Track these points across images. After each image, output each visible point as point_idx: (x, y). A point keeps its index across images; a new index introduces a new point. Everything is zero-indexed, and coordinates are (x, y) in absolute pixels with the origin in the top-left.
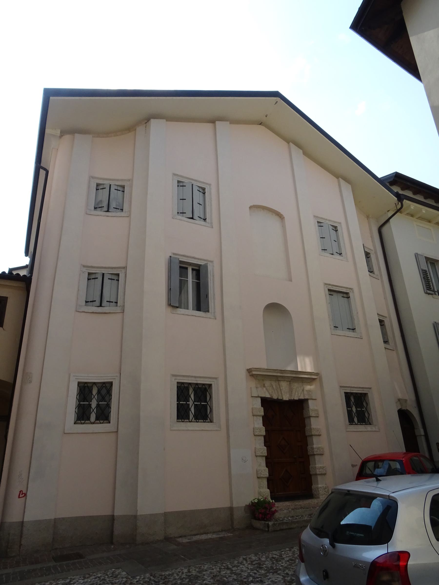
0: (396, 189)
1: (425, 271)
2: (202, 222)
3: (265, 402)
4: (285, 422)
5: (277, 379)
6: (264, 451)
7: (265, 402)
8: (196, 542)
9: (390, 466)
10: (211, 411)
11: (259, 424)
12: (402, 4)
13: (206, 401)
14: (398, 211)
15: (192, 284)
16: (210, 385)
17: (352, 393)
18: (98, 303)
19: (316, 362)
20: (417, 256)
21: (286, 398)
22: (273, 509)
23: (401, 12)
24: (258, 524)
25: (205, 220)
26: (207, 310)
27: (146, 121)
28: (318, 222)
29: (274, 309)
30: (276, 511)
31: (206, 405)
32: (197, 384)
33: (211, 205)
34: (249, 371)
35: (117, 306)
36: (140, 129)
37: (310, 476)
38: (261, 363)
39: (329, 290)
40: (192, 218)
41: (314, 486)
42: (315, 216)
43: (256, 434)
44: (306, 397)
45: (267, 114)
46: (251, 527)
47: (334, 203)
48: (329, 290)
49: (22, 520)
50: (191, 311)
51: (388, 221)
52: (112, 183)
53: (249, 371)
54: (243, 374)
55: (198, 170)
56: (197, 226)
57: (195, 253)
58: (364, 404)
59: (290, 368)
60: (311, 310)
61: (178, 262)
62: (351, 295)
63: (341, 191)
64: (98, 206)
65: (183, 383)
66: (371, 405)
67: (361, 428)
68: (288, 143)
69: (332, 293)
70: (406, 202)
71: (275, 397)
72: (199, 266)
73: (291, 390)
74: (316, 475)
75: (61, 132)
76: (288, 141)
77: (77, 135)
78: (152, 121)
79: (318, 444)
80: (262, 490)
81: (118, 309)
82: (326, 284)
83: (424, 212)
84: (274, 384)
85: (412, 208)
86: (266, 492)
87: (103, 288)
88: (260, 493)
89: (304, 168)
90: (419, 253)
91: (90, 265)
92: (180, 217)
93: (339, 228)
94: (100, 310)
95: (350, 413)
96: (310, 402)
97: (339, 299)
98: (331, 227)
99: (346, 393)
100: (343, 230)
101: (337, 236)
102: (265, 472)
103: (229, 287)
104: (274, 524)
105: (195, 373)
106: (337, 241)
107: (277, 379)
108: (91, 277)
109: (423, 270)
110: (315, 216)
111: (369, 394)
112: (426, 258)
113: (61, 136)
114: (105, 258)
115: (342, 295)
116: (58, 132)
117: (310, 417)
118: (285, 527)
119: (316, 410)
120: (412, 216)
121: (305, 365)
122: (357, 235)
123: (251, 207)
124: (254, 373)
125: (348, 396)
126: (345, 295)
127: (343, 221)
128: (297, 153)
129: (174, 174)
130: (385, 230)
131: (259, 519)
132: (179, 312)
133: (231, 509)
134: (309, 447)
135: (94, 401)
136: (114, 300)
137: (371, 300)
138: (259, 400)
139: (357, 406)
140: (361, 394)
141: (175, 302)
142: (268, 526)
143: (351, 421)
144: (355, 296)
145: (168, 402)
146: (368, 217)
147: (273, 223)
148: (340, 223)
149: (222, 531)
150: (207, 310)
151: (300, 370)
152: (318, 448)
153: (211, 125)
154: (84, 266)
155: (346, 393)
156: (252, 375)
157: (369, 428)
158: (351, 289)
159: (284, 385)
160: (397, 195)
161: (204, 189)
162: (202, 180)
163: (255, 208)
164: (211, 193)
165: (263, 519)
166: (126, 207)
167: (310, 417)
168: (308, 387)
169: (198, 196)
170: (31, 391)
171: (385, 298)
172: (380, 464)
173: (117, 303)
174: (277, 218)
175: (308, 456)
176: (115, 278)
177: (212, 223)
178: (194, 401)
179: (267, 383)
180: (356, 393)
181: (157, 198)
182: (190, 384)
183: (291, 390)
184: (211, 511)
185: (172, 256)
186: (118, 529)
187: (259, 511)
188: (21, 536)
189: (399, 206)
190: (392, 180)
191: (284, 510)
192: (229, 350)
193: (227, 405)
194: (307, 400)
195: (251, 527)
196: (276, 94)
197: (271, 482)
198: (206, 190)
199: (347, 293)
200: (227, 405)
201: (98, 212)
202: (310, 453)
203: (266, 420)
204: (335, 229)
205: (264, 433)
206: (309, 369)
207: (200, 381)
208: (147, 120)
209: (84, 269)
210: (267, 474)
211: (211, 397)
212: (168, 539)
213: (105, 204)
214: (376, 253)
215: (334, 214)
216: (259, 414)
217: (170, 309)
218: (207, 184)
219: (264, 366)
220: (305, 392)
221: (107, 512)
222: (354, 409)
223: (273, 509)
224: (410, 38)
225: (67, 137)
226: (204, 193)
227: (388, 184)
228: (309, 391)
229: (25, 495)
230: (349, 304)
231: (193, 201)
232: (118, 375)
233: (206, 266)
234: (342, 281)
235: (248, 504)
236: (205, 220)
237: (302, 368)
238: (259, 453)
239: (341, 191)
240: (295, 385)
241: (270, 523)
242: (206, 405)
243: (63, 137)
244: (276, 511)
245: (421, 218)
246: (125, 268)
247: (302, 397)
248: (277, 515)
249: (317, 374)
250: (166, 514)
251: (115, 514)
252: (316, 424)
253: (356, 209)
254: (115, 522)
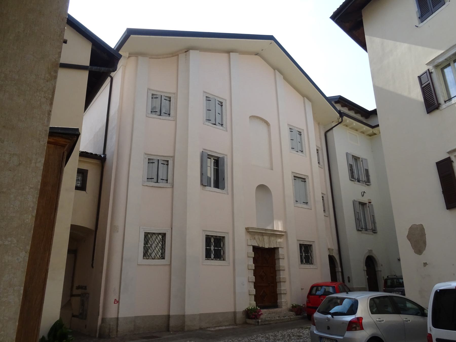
0: (338, 107)
1: (352, 165)
2: (221, 127)
3: (255, 249)
4: (265, 260)
5: (262, 234)
6: (253, 278)
7: (255, 249)
8: (220, 330)
9: (325, 289)
10: (224, 253)
11: (251, 262)
12: (363, 11)
13: (221, 247)
14: (340, 123)
15: (216, 173)
16: (224, 237)
17: (303, 244)
18: (155, 180)
19: (285, 224)
20: (347, 154)
21: (267, 246)
22: (260, 313)
23: (361, 16)
24: (249, 321)
25: (222, 125)
26: (223, 188)
27: (186, 50)
28: (290, 129)
29: (262, 188)
30: (262, 314)
31: (221, 250)
32: (216, 236)
33: (226, 115)
34: (247, 229)
35: (167, 183)
36: (182, 57)
37: (277, 295)
38: (254, 224)
39: (294, 176)
40: (215, 124)
41: (278, 301)
42: (288, 124)
43: (249, 268)
44: (278, 246)
45: (262, 48)
46: (246, 323)
47: (301, 116)
48: (294, 176)
49: (116, 317)
50: (212, 189)
51: (332, 129)
52: (163, 94)
53: (247, 229)
54: (244, 231)
55: (219, 91)
56: (217, 130)
57: (219, 149)
58: (310, 251)
59: (269, 228)
60: (283, 189)
61: (207, 155)
62: (307, 180)
63: (305, 107)
64: (153, 111)
65: (208, 235)
66: (314, 252)
67: (308, 266)
68: (274, 70)
69: (296, 178)
70: (345, 118)
71: (261, 246)
72: (218, 158)
73: (270, 242)
74: (281, 294)
75: (129, 54)
76: (274, 68)
77: (140, 58)
78: (191, 51)
79: (283, 275)
80: (251, 302)
81: (168, 185)
82: (293, 172)
83: (354, 124)
84: (261, 237)
85: (348, 122)
86: (254, 303)
87: (160, 170)
88: (250, 304)
89: (285, 90)
90: (349, 152)
91: (149, 153)
92: (207, 123)
93: (302, 133)
94: (156, 185)
95: (301, 256)
96: (280, 249)
97: (299, 182)
98: (298, 133)
99: (300, 244)
100: (304, 134)
101: (301, 139)
102: (254, 292)
103: (235, 173)
104: (262, 321)
105: (216, 230)
106: (301, 142)
107: (262, 234)
108: (150, 161)
109: (350, 165)
110: (288, 124)
111: (313, 246)
112: (352, 155)
113: (129, 57)
114: (162, 150)
115: (301, 180)
116: (127, 55)
117: (279, 259)
118: (267, 323)
119: (283, 255)
120: (347, 126)
121: (278, 226)
122: (313, 139)
123: (250, 117)
124: (250, 230)
125: (301, 246)
126: (303, 180)
127: (305, 128)
128: (279, 77)
129: (204, 92)
130: (329, 134)
131: (252, 319)
132: (206, 189)
133: (235, 313)
134: (277, 277)
135: (155, 244)
136: (165, 179)
137: (318, 184)
138: (252, 247)
139: (306, 253)
140: (308, 245)
141: (204, 183)
142: (258, 322)
143: (302, 262)
144: (309, 181)
145: (198, 247)
146: (319, 124)
147: (262, 128)
148: (303, 130)
149: (229, 325)
150: (223, 188)
151: (275, 229)
152: (283, 278)
153: (226, 55)
154: (146, 154)
155: (300, 244)
156: (249, 232)
157: (311, 266)
158: (307, 176)
159: (266, 238)
160: (340, 112)
161: (222, 103)
162: (221, 97)
163: (253, 117)
164: (227, 105)
165: (254, 319)
166: (172, 113)
167: (279, 259)
168: (279, 240)
169: (218, 107)
170: (118, 237)
171: (325, 181)
172: (319, 288)
173: (167, 180)
174: (265, 125)
175: (276, 283)
176: (166, 163)
177: (226, 128)
178: (215, 247)
179: (257, 237)
180: (306, 245)
181: (194, 109)
182: (212, 236)
183: (270, 242)
184: (224, 313)
185: (204, 151)
186: (172, 323)
187: (250, 314)
188: (117, 326)
189: (340, 120)
190: (337, 100)
191: (265, 314)
192: (233, 215)
193: (234, 250)
194: (278, 248)
195: (246, 323)
196: (271, 38)
197: (257, 298)
198: (223, 104)
199: (304, 179)
200: (234, 250)
201: (154, 116)
202: (278, 280)
203: (255, 260)
204: (300, 134)
205: (254, 268)
206: (280, 229)
207: (219, 235)
208: (187, 51)
209: (146, 156)
210: (254, 293)
211: (224, 245)
212: (201, 329)
213: (158, 110)
214: (322, 150)
215: (301, 125)
216: (251, 256)
217: (202, 187)
218: (224, 99)
219: (255, 226)
220: (278, 243)
221: (164, 312)
222: (304, 254)
223: (260, 313)
224: (366, 36)
225: (133, 59)
226: (222, 106)
227: (333, 103)
228: (280, 242)
229: (118, 302)
230: (305, 186)
231: (216, 113)
232: (170, 229)
233: (223, 158)
234: (303, 171)
235: (244, 310)
236: (222, 125)
237: (276, 228)
238: (250, 280)
239: (305, 110)
240: (272, 239)
241: (260, 321)
242: (221, 250)
243: (131, 58)
244: (262, 314)
245: (352, 128)
246: (173, 157)
247: (276, 247)
248: (262, 316)
249: (285, 232)
250: (201, 315)
251: (171, 314)
252: (283, 263)
253: (314, 120)
254: (171, 319)
